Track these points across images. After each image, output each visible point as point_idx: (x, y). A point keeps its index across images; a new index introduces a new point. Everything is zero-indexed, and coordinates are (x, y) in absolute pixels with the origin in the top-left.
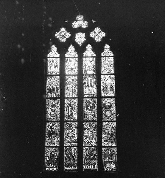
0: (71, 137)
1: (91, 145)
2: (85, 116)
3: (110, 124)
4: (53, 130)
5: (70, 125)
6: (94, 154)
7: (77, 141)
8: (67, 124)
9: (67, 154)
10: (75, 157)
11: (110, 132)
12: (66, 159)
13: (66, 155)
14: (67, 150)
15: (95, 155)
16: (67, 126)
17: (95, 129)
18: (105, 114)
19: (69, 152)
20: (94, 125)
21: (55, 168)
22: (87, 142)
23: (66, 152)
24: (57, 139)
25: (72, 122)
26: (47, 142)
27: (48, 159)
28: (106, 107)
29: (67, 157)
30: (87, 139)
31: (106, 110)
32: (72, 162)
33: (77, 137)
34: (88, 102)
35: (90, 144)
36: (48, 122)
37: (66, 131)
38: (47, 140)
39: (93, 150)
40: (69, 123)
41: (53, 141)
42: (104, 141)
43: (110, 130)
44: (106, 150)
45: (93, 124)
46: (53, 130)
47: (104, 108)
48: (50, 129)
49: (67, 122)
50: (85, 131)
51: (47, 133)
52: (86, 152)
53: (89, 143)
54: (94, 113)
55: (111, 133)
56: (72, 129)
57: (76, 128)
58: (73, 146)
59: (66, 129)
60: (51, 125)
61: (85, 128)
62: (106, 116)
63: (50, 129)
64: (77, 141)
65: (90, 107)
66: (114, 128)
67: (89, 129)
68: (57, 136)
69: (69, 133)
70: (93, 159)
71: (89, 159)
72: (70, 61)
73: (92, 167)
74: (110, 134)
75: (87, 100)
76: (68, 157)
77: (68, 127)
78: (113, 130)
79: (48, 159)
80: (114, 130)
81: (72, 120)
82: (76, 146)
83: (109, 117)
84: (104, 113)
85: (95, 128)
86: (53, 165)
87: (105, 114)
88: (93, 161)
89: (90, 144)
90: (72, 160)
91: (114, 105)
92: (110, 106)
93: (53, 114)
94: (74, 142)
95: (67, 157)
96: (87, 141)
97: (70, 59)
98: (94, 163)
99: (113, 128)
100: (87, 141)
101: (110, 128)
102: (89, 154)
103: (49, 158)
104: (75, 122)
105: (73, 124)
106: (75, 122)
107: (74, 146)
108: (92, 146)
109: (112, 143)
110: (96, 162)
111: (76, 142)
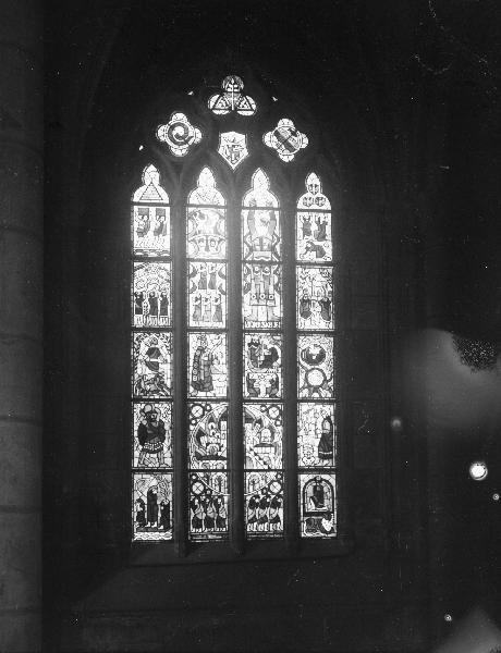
0: (207, 444)
1: (266, 467)
2: (249, 384)
3: (319, 407)
4: (154, 424)
5: (204, 409)
6: (276, 491)
7: (225, 455)
8: (197, 408)
9: (198, 492)
10: (220, 501)
11: (318, 432)
12: (195, 508)
13: (195, 495)
14: (196, 481)
15: (278, 495)
16: (196, 411)
17: (278, 423)
18: (306, 380)
19: (202, 488)
20: (274, 409)
21: (160, 531)
22: (253, 459)
23: (194, 488)
24: (165, 449)
25: (212, 400)
26: (136, 461)
27: (140, 509)
28: (309, 359)
29: (197, 501)
30: (256, 450)
31: (309, 367)
32: (211, 515)
33: (225, 445)
34: (257, 345)
35: (265, 463)
36: (138, 400)
37: (192, 427)
38: (137, 454)
39: (272, 481)
40: (200, 405)
41: (155, 456)
42: (302, 455)
43: (319, 426)
44: (310, 481)
45: (273, 406)
46: (154, 424)
47: (302, 362)
48: (145, 423)
49: (196, 401)
50: (248, 426)
51: (136, 434)
52: (251, 487)
53: (261, 462)
54: (274, 377)
55: (323, 434)
56: (211, 420)
57: (224, 417)
58: (213, 471)
59: (194, 422)
60: (148, 408)
61: (249, 420)
62: (309, 386)
63: (145, 423)
64: (225, 455)
65: (262, 358)
66: (332, 418)
67: (260, 421)
68: (166, 441)
69: (201, 434)
70: (275, 505)
71: (263, 505)
72: (202, 216)
73: (268, 526)
74: (320, 436)
75: (256, 338)
76: (199, 502)
77: (197, 415)
78: (327, 425)
79: (140, 509)
80: (331, 424)
81: (209, 394)
82: (223, 470)
83: (316, 389)
84: (301, 377)
85: (277, 419)
86: (155, 525)
87: (306, 380)
88: (272, 510)
89: (265, 463)
90: (210, 510)
91: (329, 355)
92: (321, 356)
93: (153, 376)
94: (217, 458)
95: (197, 501)
96: (256, 454)
97: (203, 210)
98: (274, 516)
99: (328, 418)
100: (256, 454)
101: (321, 419)
102: (260, 493)
103: (142, 505)
104: (217, 401)
105: (214, 406)
106: (217, 401)
107: (216, 471)
108: (269, 470)
109: (326, 462)
110: (280, 512)
111: (223, 459)
